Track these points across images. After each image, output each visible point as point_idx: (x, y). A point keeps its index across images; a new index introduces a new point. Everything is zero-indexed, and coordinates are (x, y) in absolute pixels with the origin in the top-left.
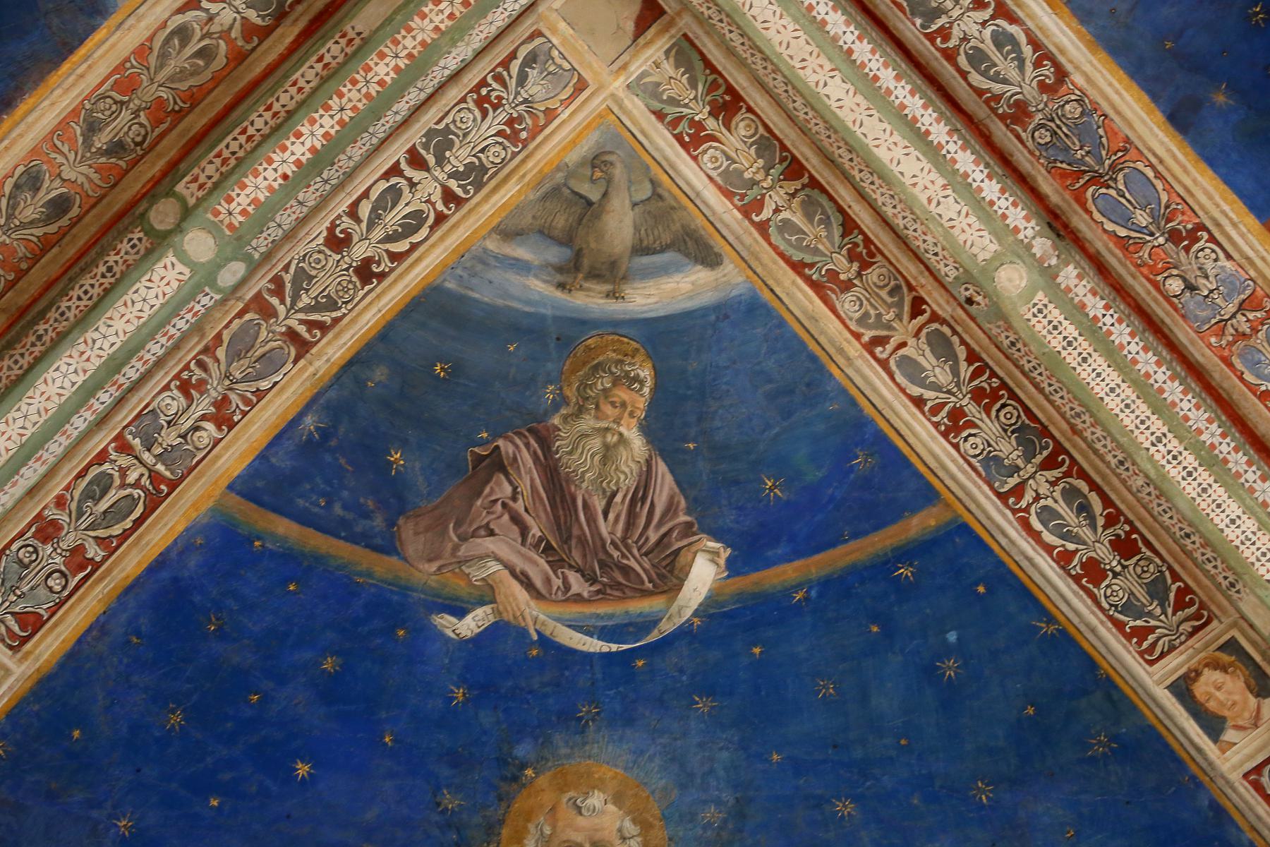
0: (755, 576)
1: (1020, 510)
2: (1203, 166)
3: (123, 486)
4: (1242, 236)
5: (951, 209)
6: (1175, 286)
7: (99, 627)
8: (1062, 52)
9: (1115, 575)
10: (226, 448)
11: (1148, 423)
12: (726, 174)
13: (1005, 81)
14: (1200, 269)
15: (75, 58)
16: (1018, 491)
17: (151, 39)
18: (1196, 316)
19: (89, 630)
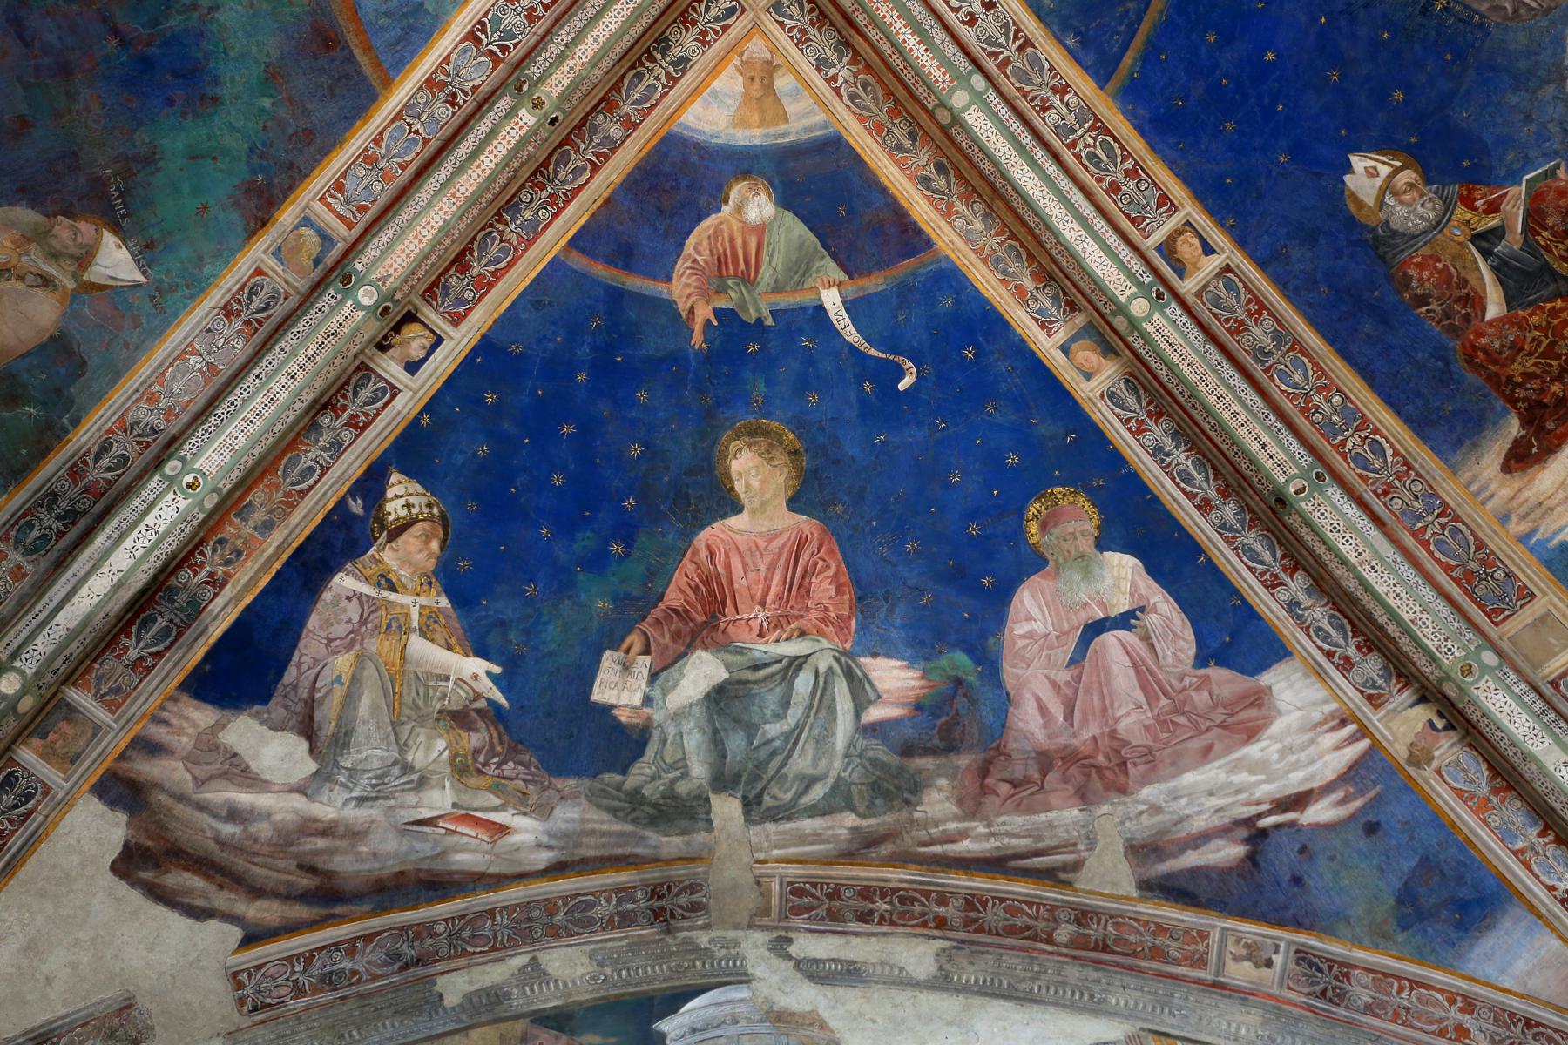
3: (1094, 146)
7: (1171, 165)
10: (1080, 89)
15: (862, 155)
17: (855, 114)
19: (1171, 169)
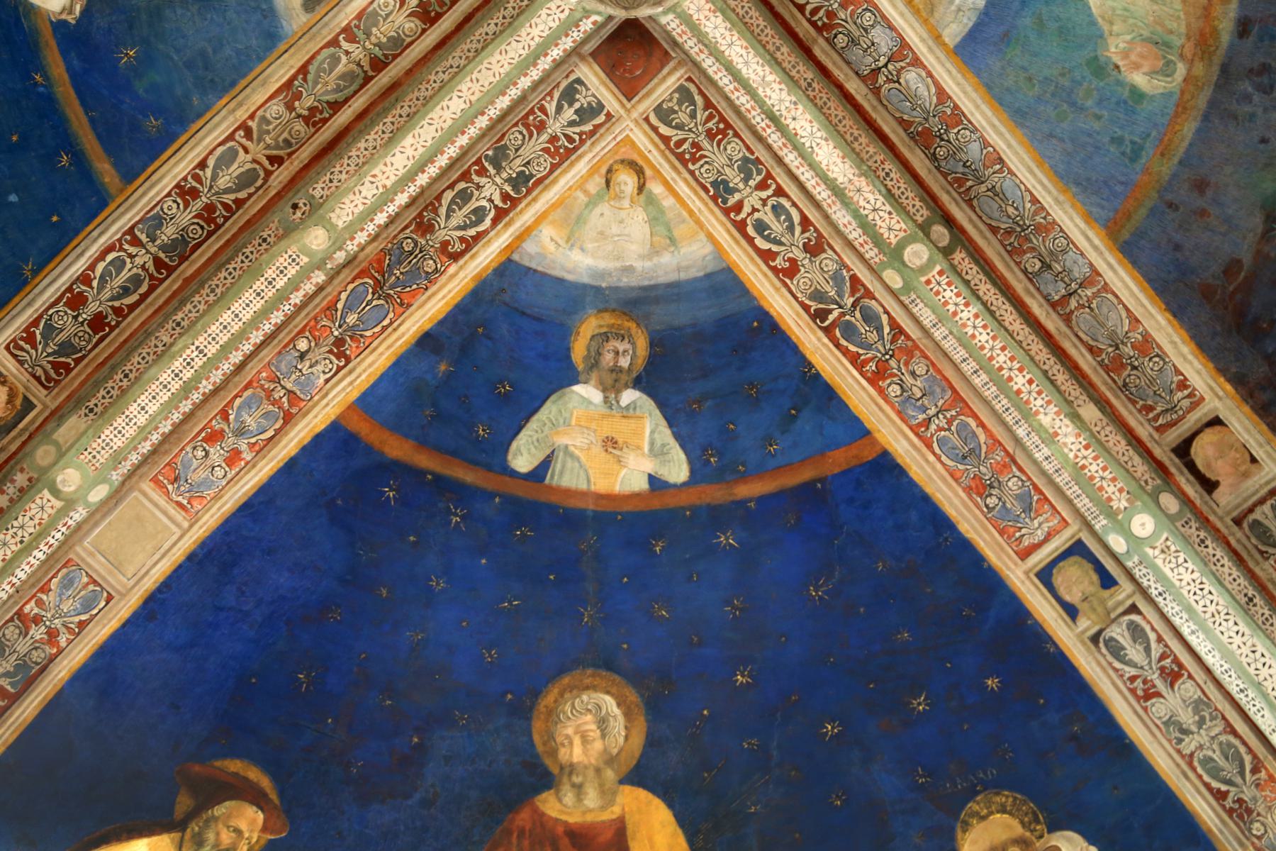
0: (53, 43)
1: (121, 245)
2: (394, 359)
4: (344, 389)
5: (369, 191)
6: (303, 345)
8: (473, 257)
9: (75, 318)
11: (213, 343)
12: (375, 13)
13: (448, 217)
14: (317, 362)
16: (136, 242)
18: (281, 361)
